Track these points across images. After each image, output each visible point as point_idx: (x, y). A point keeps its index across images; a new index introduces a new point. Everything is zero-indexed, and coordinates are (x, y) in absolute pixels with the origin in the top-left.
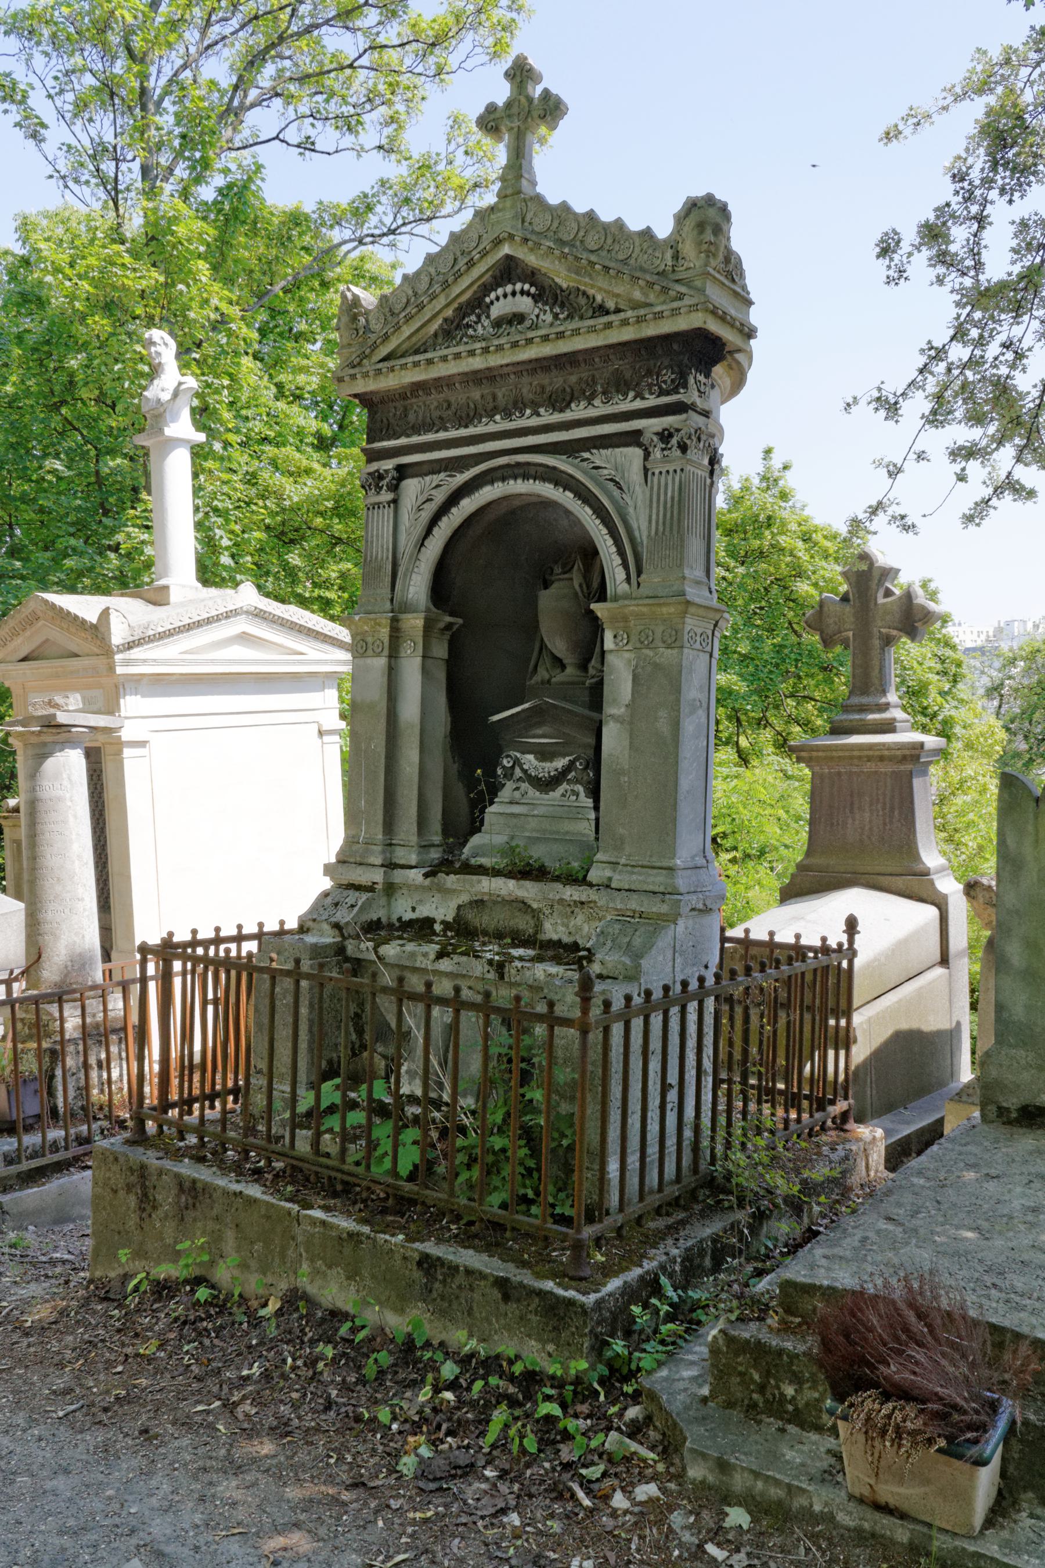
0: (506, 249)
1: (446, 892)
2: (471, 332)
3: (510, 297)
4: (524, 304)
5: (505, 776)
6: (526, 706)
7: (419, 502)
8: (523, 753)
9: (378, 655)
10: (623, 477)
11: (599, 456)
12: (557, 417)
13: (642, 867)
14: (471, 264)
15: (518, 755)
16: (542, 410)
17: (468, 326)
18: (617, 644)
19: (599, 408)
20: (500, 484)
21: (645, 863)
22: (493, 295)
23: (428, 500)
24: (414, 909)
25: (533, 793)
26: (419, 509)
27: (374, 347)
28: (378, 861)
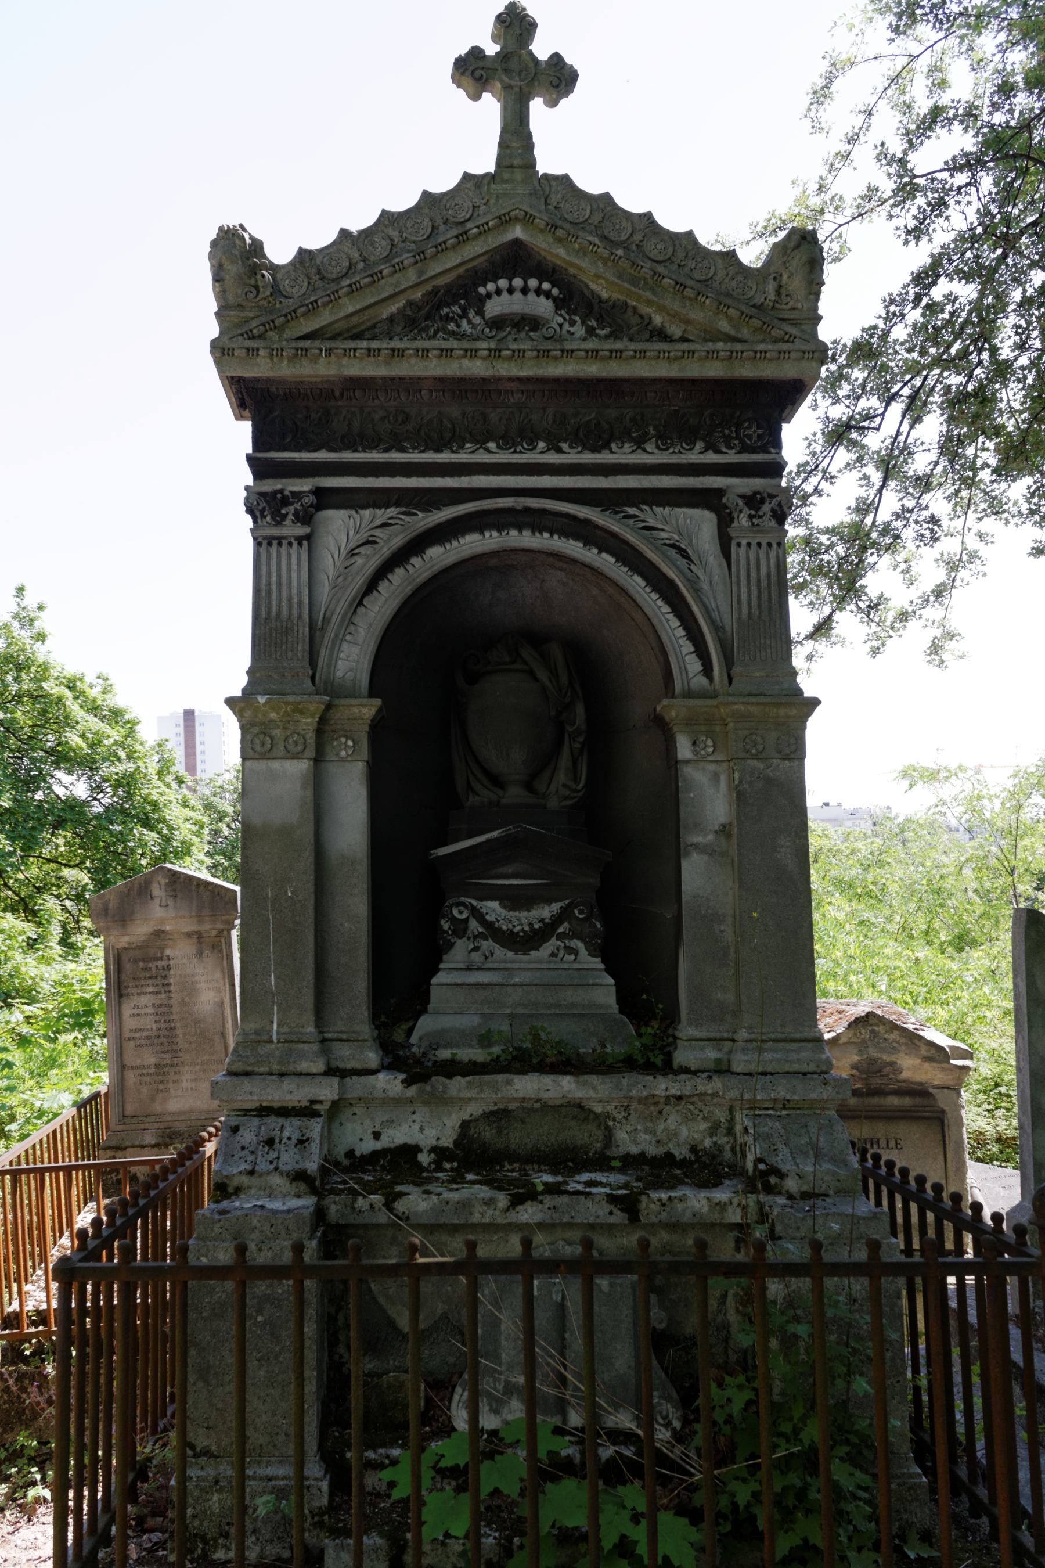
0: (518, 232)
1: (440, 1102)
2: (452, 326)
3: (505, 294)
4: (543, 307)
5: (454, 932)
6: (495, 834)
7: (352, 545)
8: (481, 899)
9: (296, 756)
10: (690, 544)
11: (654, 515)
12: (588, 458)
13: (775, 1040)
14: (463, 238)
15: (474, 903)
16: (565, 446)
17: (448, 319)
18: (696, 753)
19: (652, 456)
20: (495, 534)
21: (780, 1036)
22: (491, 286)
23: (367, 542)
24: (377, 1135)
26: (352, 553)
27: (292, 316)
28: (319, 1066)
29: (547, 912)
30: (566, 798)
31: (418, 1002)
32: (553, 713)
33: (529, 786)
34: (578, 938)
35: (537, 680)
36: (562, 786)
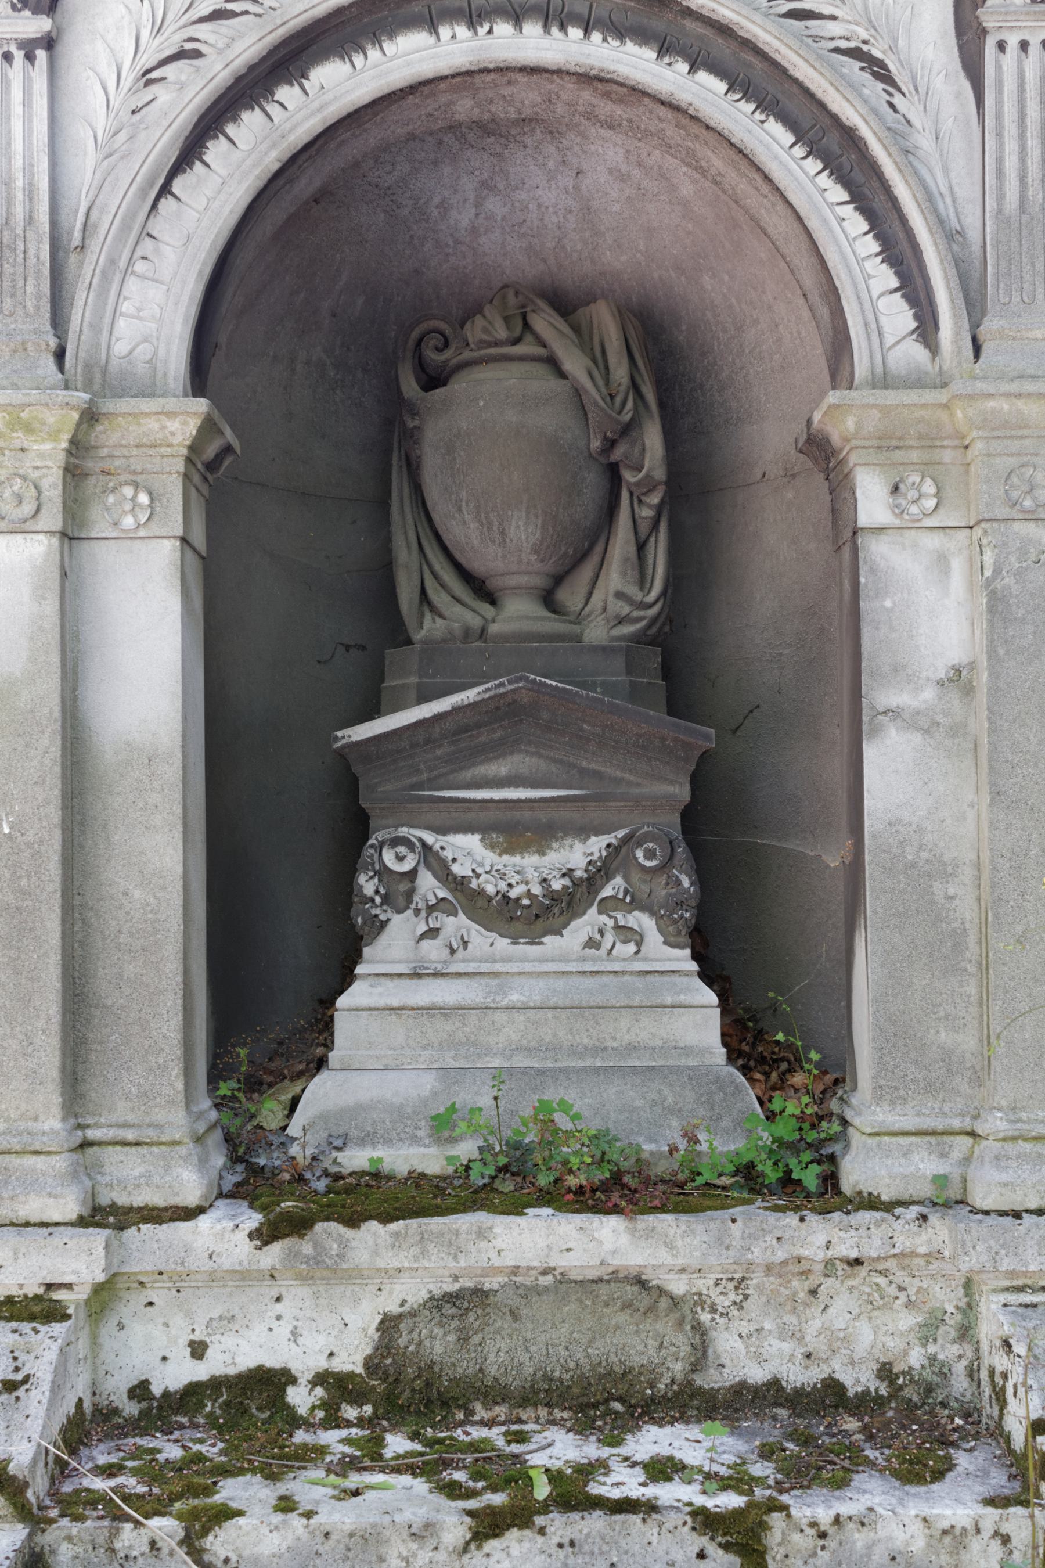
5: (386, 899)
6: (469, 695)
7: (147, 59)
8: (442, 830)
15: (429, 838)
18: (899, 511)
20: (462, 31)
24: (198, 1350)
25: (485, 943)
26: (147, 78)
28: (69, 1207)
29: (577, 855)
30: (621, 621)
31: (308, 1045)
32: (596, 444)
33: (548, 599)
34: (643, 908)
35: (562, 375)
36: (616, 596)
